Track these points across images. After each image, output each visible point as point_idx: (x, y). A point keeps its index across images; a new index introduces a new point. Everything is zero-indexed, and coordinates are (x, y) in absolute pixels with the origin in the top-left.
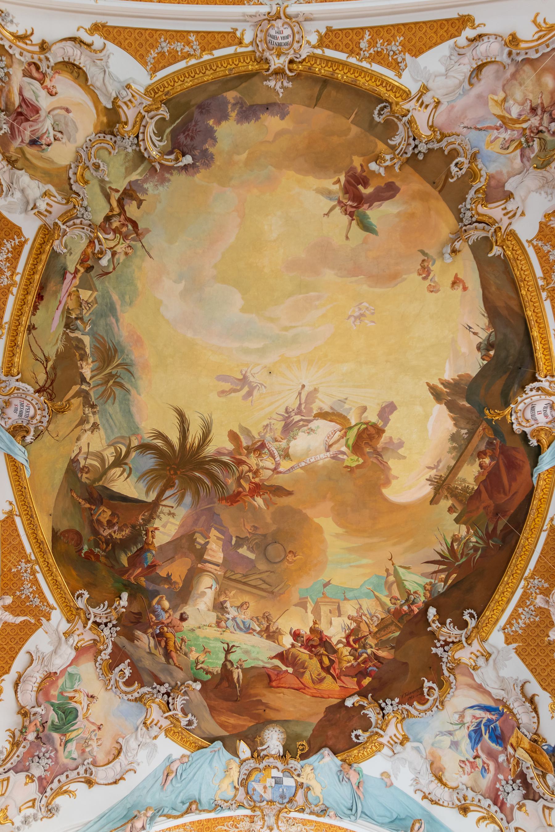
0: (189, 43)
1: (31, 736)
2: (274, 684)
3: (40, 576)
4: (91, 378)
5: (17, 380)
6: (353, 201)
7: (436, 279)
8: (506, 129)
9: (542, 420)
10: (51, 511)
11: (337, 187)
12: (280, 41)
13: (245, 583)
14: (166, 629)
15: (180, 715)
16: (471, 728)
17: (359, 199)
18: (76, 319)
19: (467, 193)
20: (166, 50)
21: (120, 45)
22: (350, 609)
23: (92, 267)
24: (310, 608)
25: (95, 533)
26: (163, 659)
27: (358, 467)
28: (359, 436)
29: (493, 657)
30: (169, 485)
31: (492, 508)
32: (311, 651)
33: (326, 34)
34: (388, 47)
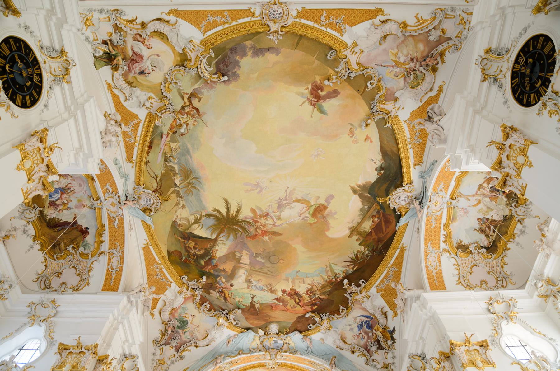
0: (224, 16)
1: (169, 332)
2: (274, 309)
3: (164, 270)
4: (180, 185)
5: (143, 188)
6: (315, 98)
7: (357, 137)
8: (397, 67)
9: (403, 203)
10: (166, 243)
11: (307, 91)
12: (276, 16)
13: (260, 272)
14: (224, 290)
15: (233, 321)
16: (359, 324)
17: (318, 98)
18: (170, 157)
19: (375, 96)
21: (185, 19)
22: (309, 281)
23: (176, 131)
24: (290, 281)
25: (188, 252)
26: (224, 301)
27: (314, 223)
28: (315, 210)
29: (371, 298)
30: (222, 231)
31: (376, 239)
32: (291, 297)
34: (337, 21)
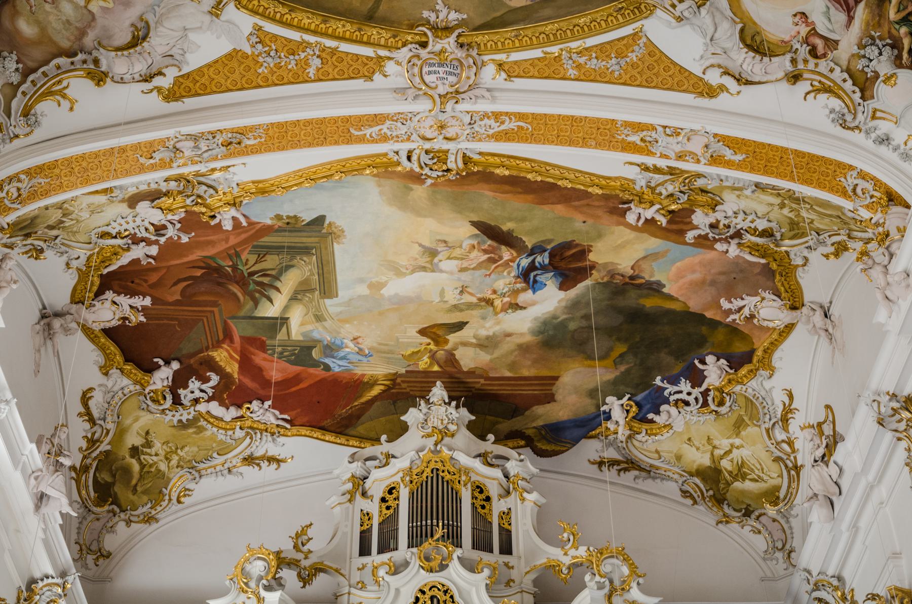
0: (579, 67)
12: (441, 70)
20: (614, 61)
21: (682, 70)
33: (373, 73)
34: (279, 60)
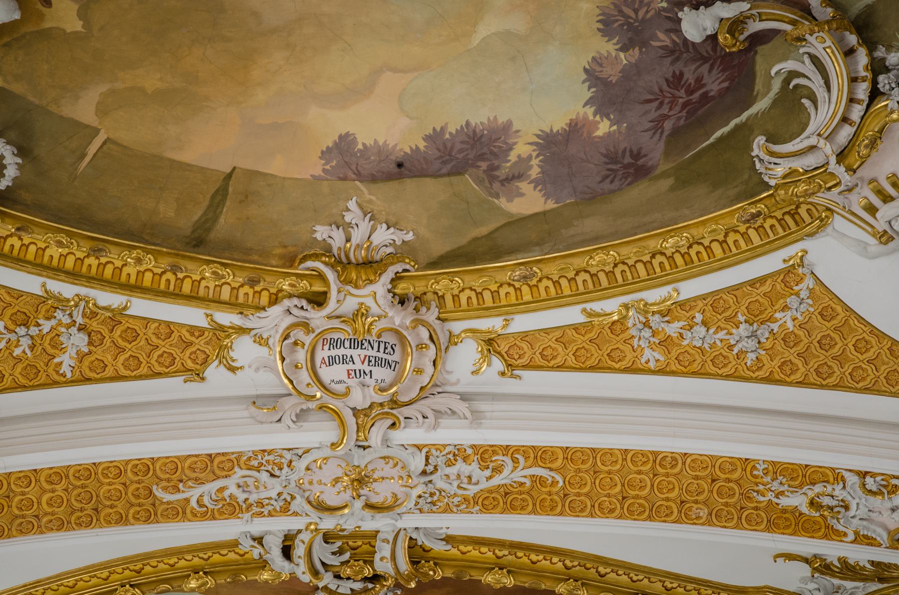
0: (666, 343)
12: (356, 353)
20: (744, 330)
33: (205, 362)
